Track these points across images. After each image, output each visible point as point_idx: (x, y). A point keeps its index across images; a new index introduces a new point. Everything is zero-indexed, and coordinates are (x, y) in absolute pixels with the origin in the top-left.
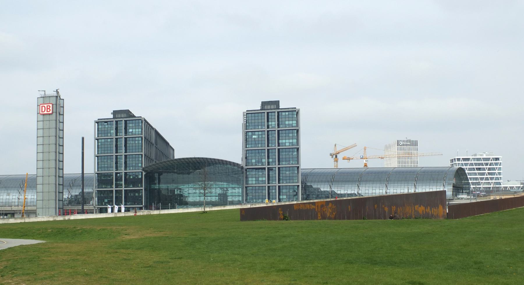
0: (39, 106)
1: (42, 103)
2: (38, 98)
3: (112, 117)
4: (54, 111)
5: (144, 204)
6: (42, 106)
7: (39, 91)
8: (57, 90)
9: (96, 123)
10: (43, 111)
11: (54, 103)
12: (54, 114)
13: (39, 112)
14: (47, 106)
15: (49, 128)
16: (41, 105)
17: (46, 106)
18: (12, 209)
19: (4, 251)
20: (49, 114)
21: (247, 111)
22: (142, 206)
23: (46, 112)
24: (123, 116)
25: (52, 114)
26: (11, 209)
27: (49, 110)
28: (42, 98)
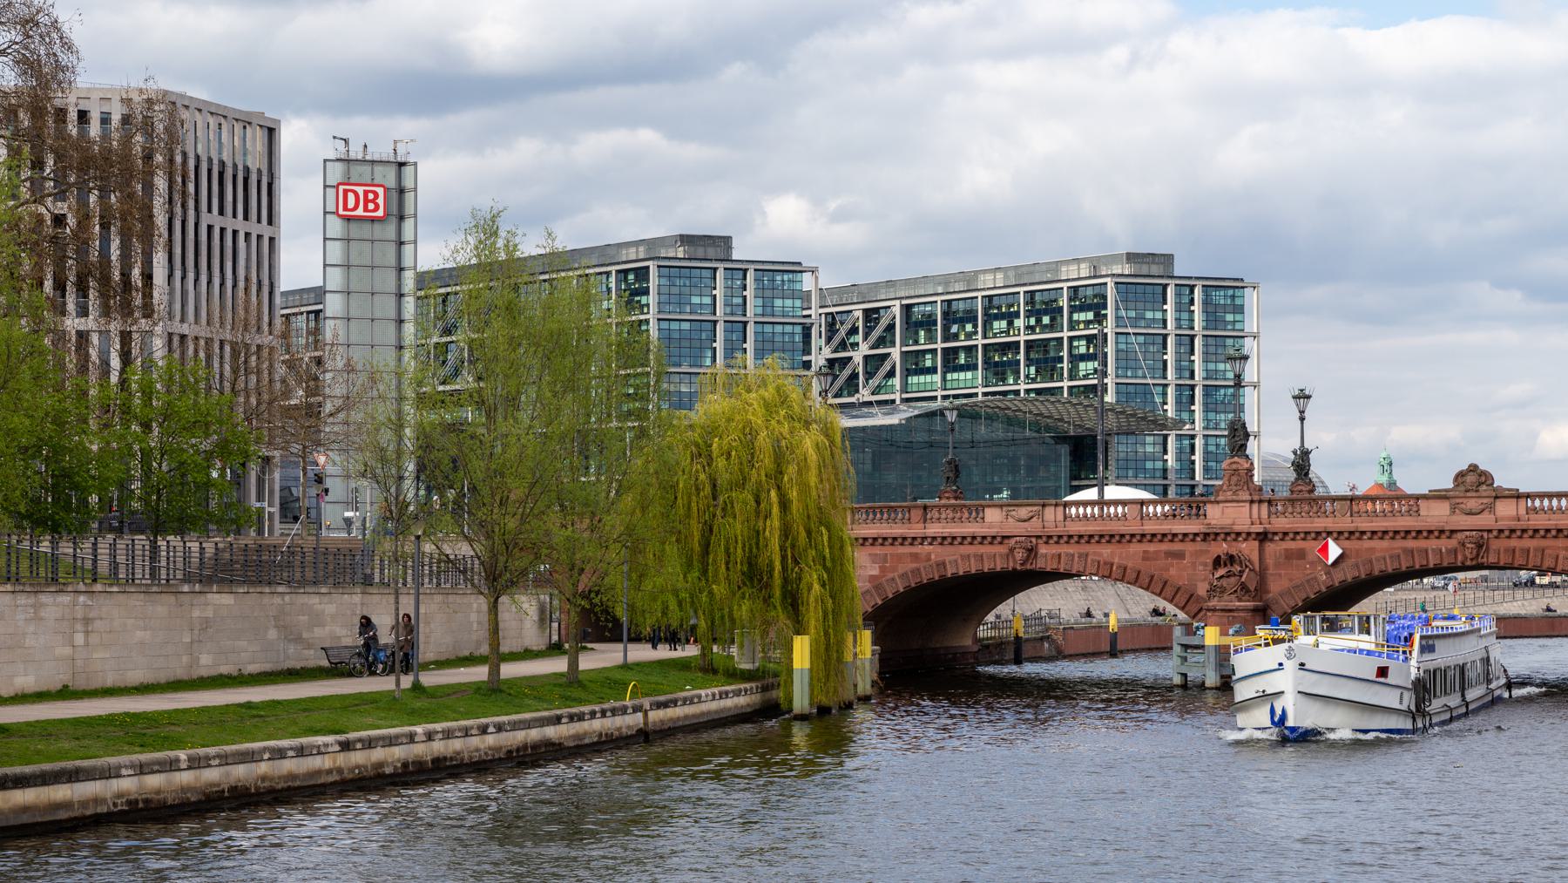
0: (335, 190)
2: (325, 161)
4: (394, 210)
6: (346, 192)
7: (334, 137)
8: (395, 142)
10: (351, 204)
11: (391, 182)
12: (394, 220)
14: (366, 193)
15: (373, 268)
16: (341, 188)
17: (360, 190)
19: (1566, 636)
20: (373, 220)
23: (360, 212)
24: (711, 253)
28: (338, 164)
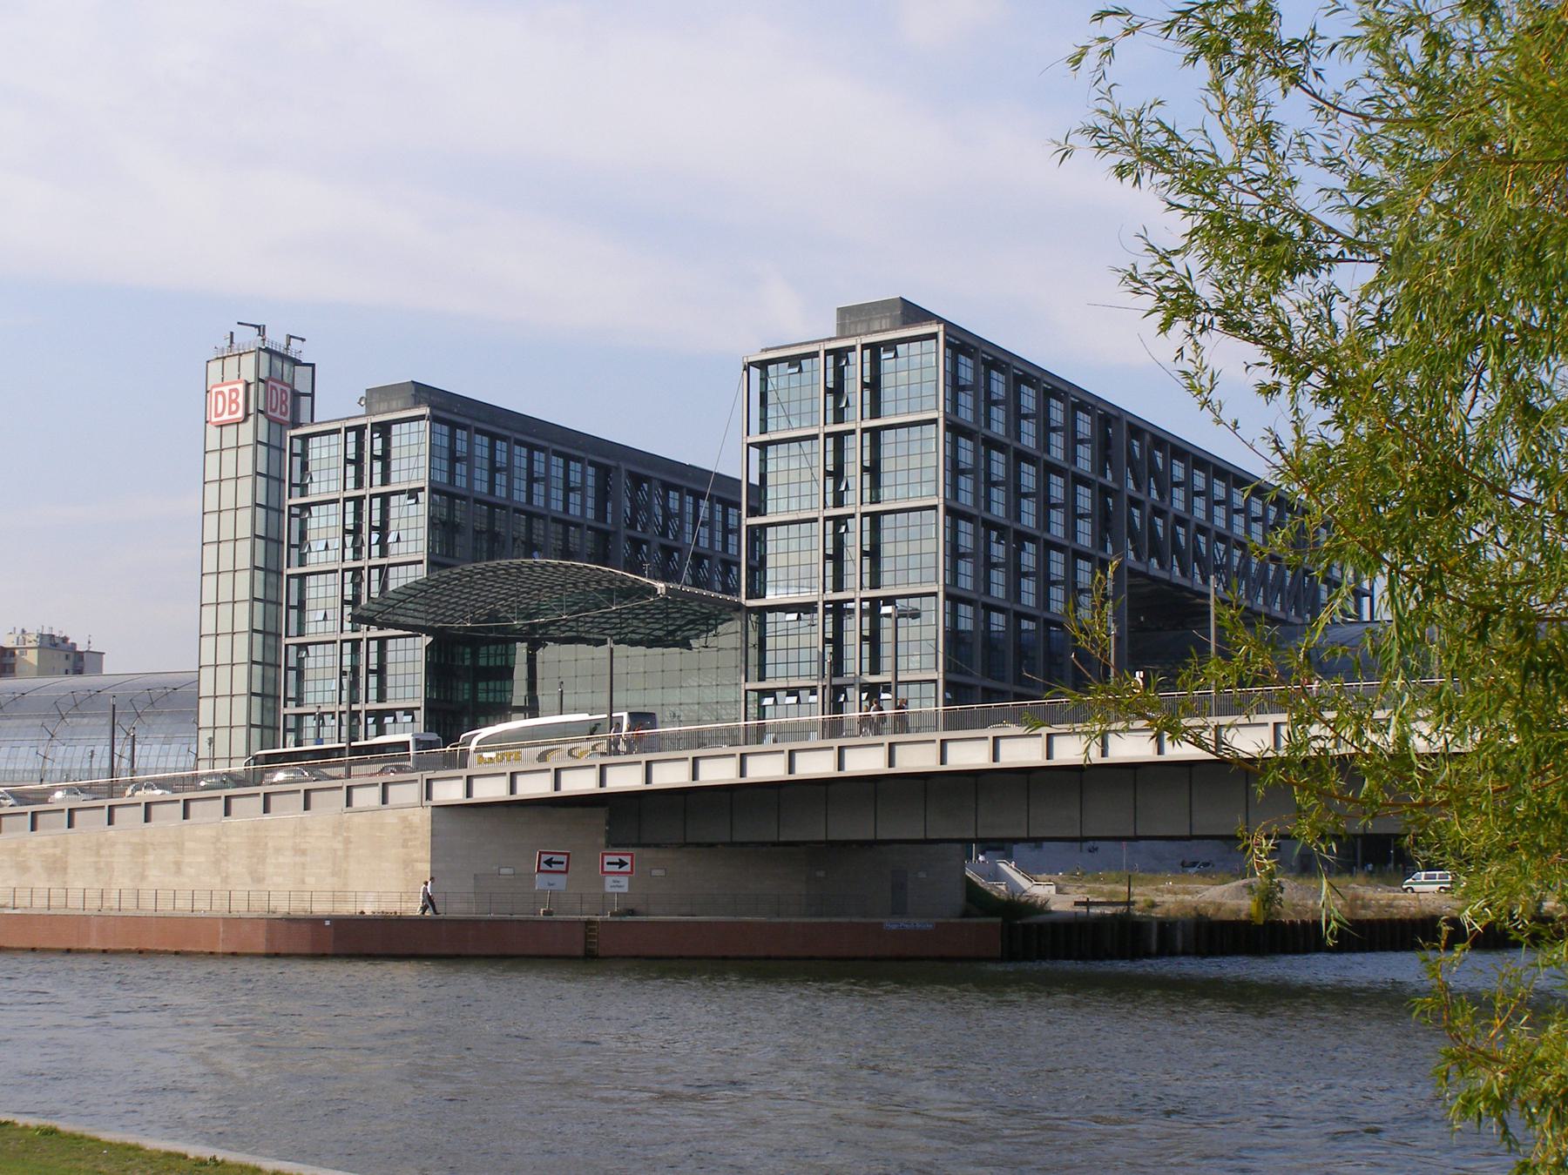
3: (364, 413)
6: (217, 393)
10: (220, 411)
11: (251, 379)
14: (231, 391)
16: (214, 390)
17: (226, 389)
20: (238, 423)
21: (762, 350)
23: (226, 417)
25: (245, 420)
27: (234, 407)
28: (220, 362)
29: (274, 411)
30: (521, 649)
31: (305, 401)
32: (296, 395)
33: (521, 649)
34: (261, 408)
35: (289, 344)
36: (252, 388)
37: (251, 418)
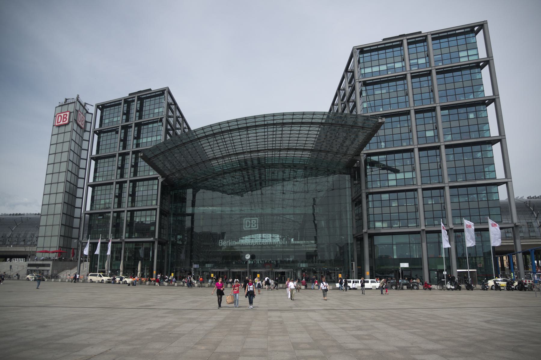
1: (60, 112)
2: (56, 107)
5: (157, 237)
6: (59, 116)
9: (98, 110)
10: (59, 121)
13: (54, 125)
14: (64, 115)
16: (58, 115)
17: (62, 115)
18: (26, 250)
20: (65, 125)
22: (152, 239)
23: (61, 123)
26: (24, 250)
28: (61, 107)
29: (80, 122)
30: (190, 191)
31: (88, 125)
32: (86, 122)
33: (190, 191)
34: (75, 119)
35: (85, 106)
36: (72, 114)
37: (71, 123)
